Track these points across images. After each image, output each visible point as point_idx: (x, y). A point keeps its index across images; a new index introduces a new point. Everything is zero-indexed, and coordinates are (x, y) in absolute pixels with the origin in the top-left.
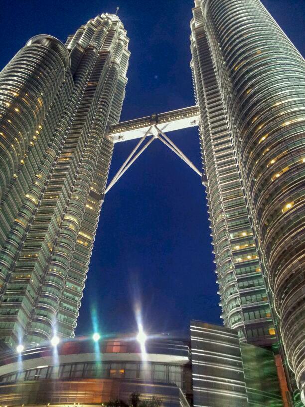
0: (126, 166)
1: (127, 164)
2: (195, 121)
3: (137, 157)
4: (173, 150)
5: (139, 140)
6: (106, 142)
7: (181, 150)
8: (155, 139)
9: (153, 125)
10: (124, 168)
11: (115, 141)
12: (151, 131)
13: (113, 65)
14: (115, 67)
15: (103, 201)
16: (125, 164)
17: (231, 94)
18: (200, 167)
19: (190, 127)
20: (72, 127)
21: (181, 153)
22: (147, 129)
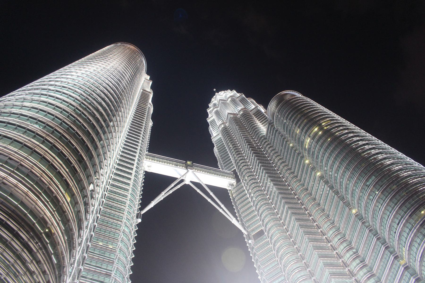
3: (171, 192)
4: (209, 200)
7: (223, 203)
8: (185, 184)
9: (190, 171)
10: (161, 198)
15: (140, 220)
16: (163, 193)
21: (222, 206)
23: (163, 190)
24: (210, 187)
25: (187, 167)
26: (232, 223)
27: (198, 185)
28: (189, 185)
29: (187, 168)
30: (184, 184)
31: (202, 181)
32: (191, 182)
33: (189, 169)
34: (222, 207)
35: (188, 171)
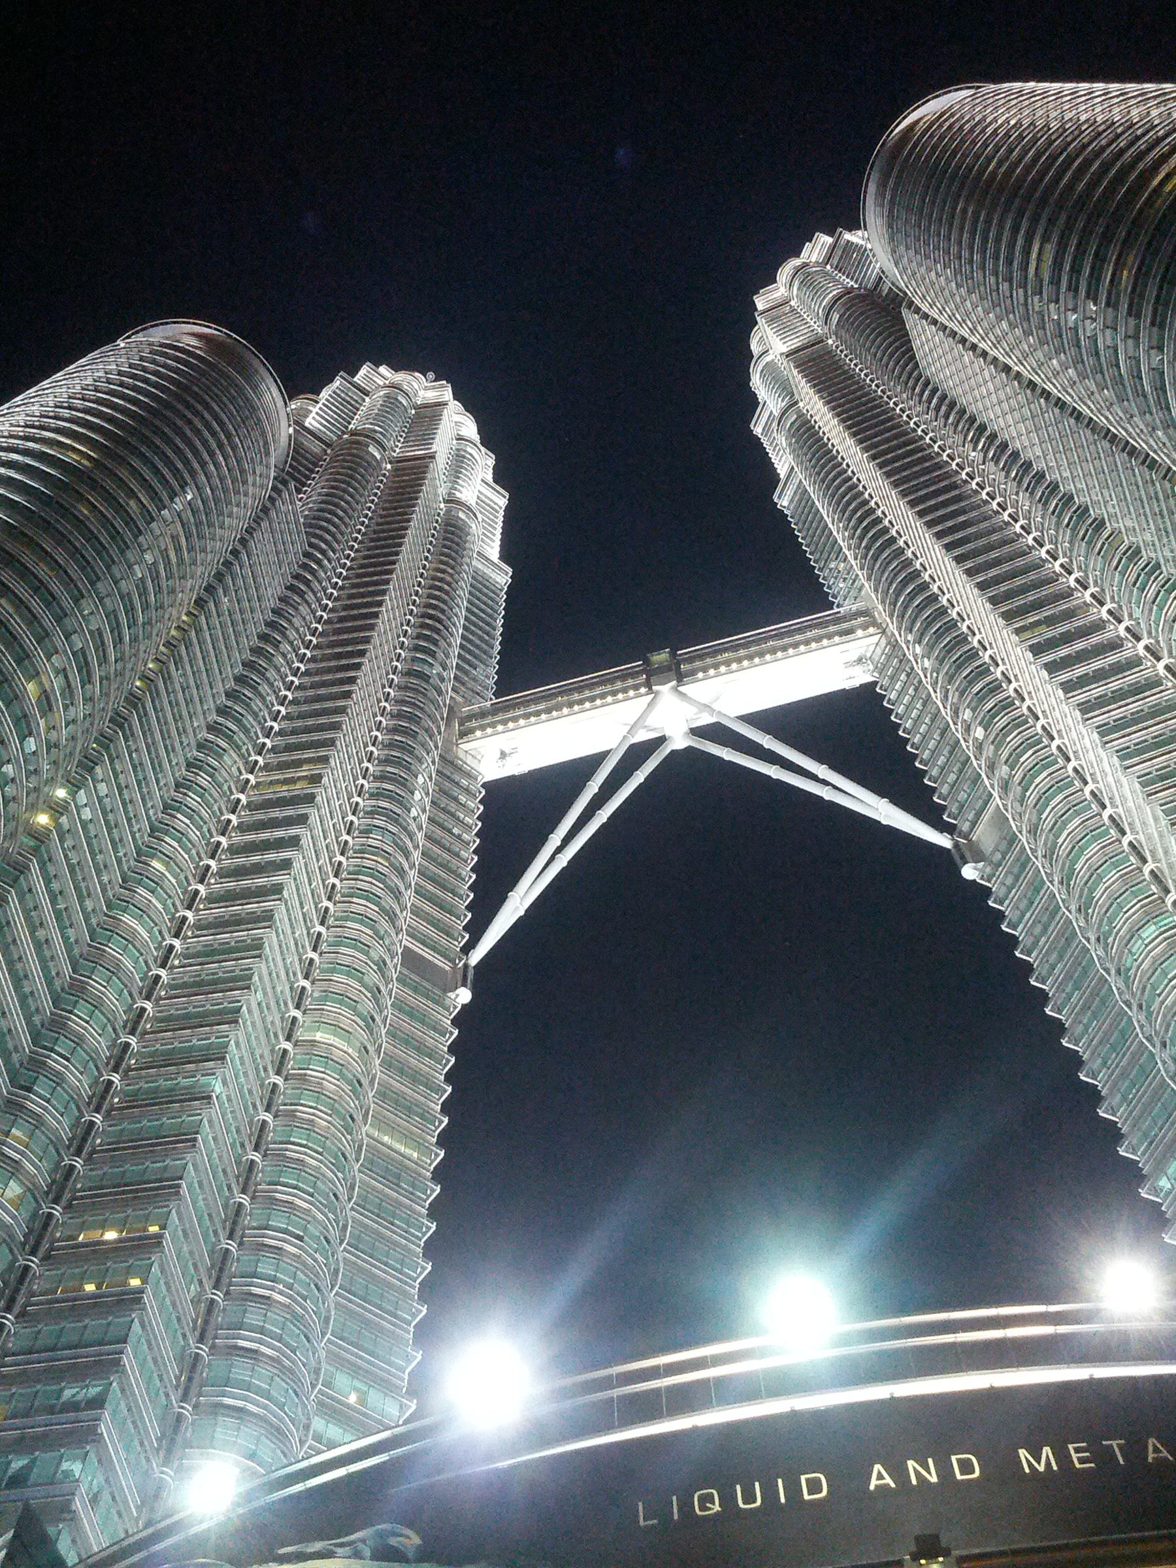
0: (559, 850)
1: (567, 841)
3: (603, 816)
5: (598, 759)
6: (451, 769)
7: (820, 760)
9: (665, 689)
13: (448, 511)
14: (462, 515)
15: (464, 996)
16: (555, 839)
17: (926, 660)
18: (932, 815)
20: (264, 777)
21: (822, 771)
24: (750, 719)
25: (652, 677)
26: (884, 822)
27: (717, 732)
28: (689, 749)
29: (648, 685)
30: (668, 751)
31: (717, 710)
32: (696, 732)
34: (821, 777)
35: (657, 693)
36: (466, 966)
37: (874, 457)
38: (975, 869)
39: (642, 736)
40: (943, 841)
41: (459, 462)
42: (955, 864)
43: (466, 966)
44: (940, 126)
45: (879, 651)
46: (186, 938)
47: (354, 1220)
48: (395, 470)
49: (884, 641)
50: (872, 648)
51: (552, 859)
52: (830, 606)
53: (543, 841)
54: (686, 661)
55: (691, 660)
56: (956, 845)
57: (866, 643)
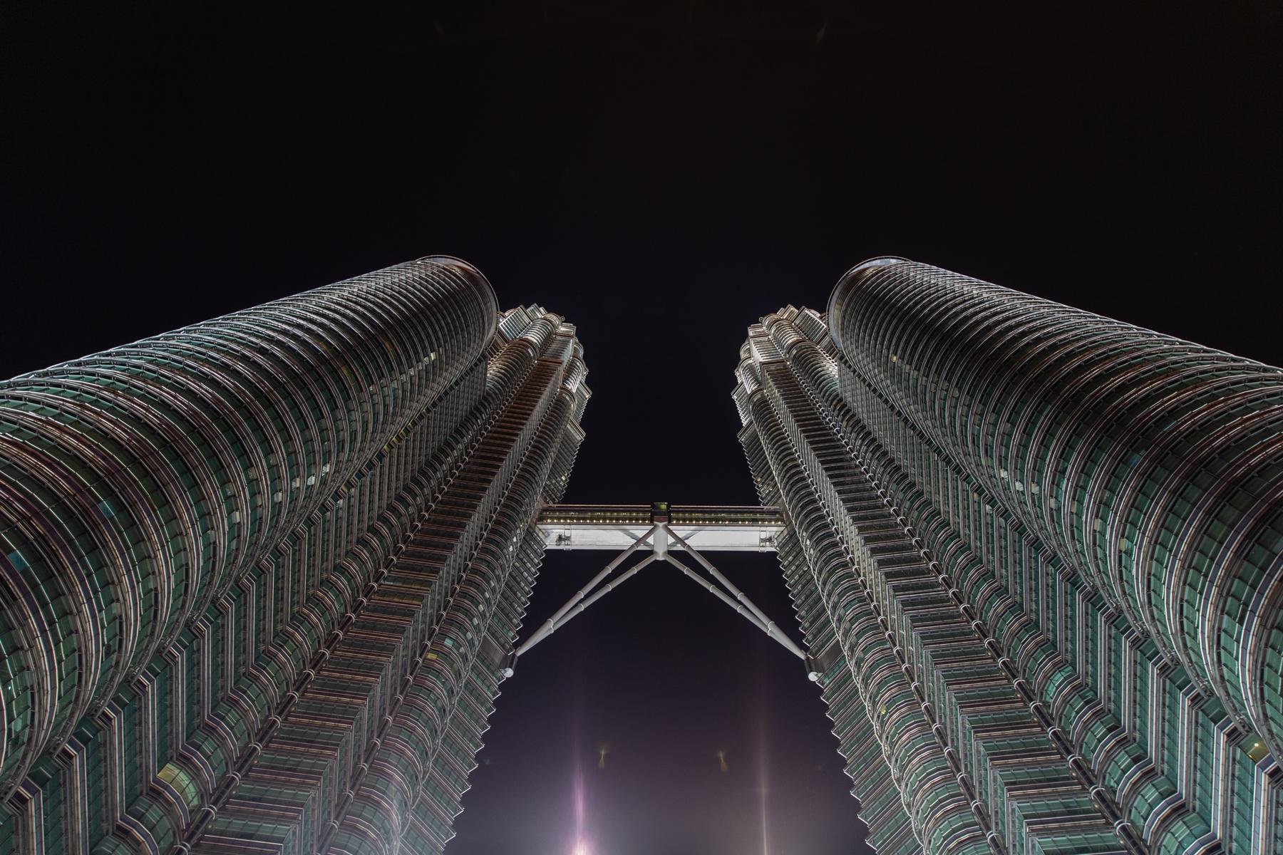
2: (770, 540)
3: (610, 588)
4: (711, 589)
6: (530, 535)
7: (741, 589)
8: (656, 561)
9: (661, 525)
11: (551, 544)
12: (650, 540)
13: (561, 393)
15: (509, 673)
16: (581, 595)
18: (797, 638)
19: (757, 552)
21: (740, 596)
22: (640, 531)
23: (581, 587)
27: (684, 557)
29: (652, 520)
30: (653, 560)
32: (670, 553)
33: (655, 523)
34: (739, 598)
35: (656, 526)
36: (514, 655)
37: (804, 431)
38: (816, 675)
39: (642, 547)
40: (801, 655)
41: (570, 370)
42: (805, 670)
43: (514, 655)
44: (883, 275)
45: (782, 536)
46: (371, 599)
47: (422, 797)
48: (539, 365)
49: (786, 532)
50: (778, 533)
51: (576, 605)
52: (759, 503)
53: (574, 593)
54: (674, 512)
55: (678, 512)
56: (808, 659)
57: (773, 530)
